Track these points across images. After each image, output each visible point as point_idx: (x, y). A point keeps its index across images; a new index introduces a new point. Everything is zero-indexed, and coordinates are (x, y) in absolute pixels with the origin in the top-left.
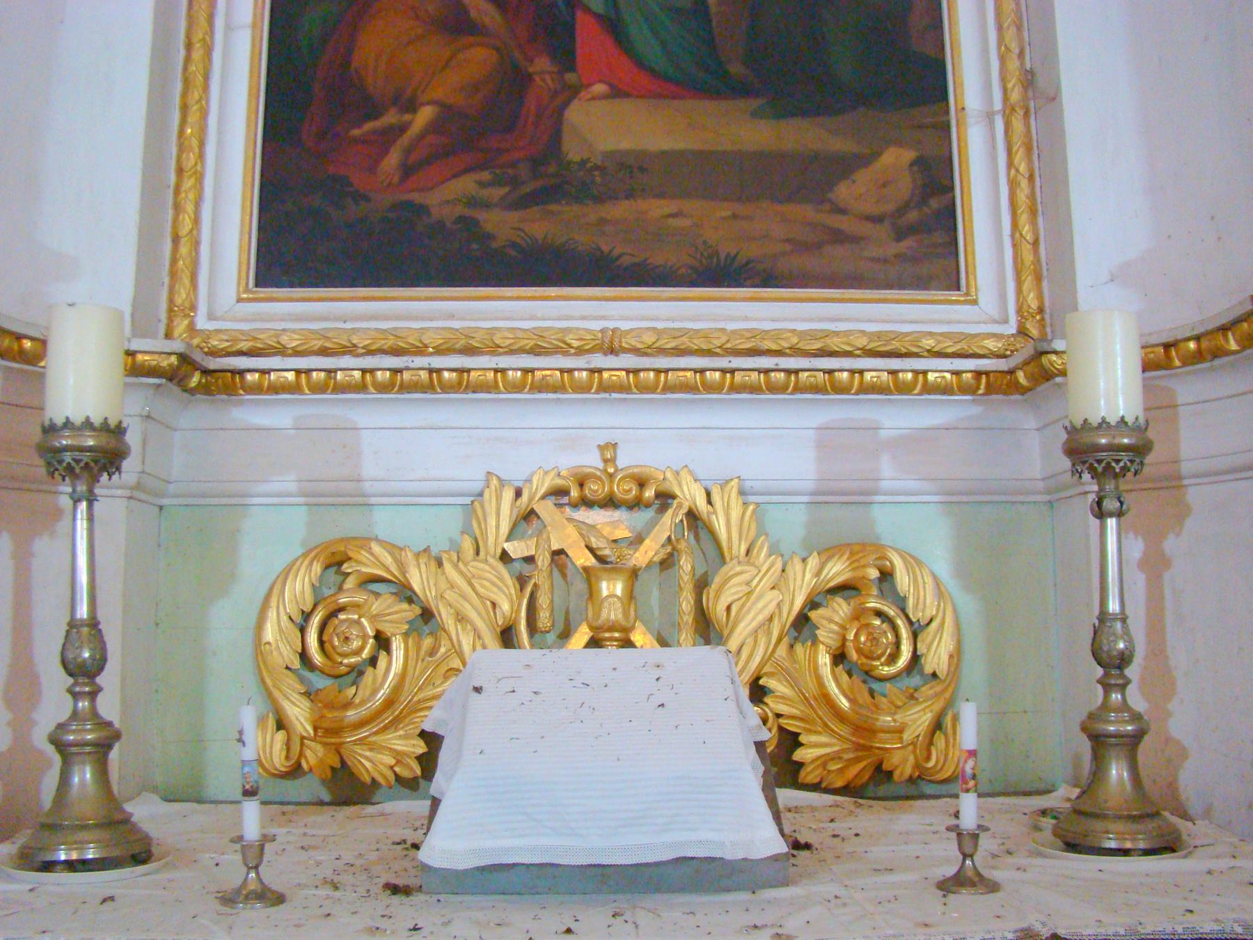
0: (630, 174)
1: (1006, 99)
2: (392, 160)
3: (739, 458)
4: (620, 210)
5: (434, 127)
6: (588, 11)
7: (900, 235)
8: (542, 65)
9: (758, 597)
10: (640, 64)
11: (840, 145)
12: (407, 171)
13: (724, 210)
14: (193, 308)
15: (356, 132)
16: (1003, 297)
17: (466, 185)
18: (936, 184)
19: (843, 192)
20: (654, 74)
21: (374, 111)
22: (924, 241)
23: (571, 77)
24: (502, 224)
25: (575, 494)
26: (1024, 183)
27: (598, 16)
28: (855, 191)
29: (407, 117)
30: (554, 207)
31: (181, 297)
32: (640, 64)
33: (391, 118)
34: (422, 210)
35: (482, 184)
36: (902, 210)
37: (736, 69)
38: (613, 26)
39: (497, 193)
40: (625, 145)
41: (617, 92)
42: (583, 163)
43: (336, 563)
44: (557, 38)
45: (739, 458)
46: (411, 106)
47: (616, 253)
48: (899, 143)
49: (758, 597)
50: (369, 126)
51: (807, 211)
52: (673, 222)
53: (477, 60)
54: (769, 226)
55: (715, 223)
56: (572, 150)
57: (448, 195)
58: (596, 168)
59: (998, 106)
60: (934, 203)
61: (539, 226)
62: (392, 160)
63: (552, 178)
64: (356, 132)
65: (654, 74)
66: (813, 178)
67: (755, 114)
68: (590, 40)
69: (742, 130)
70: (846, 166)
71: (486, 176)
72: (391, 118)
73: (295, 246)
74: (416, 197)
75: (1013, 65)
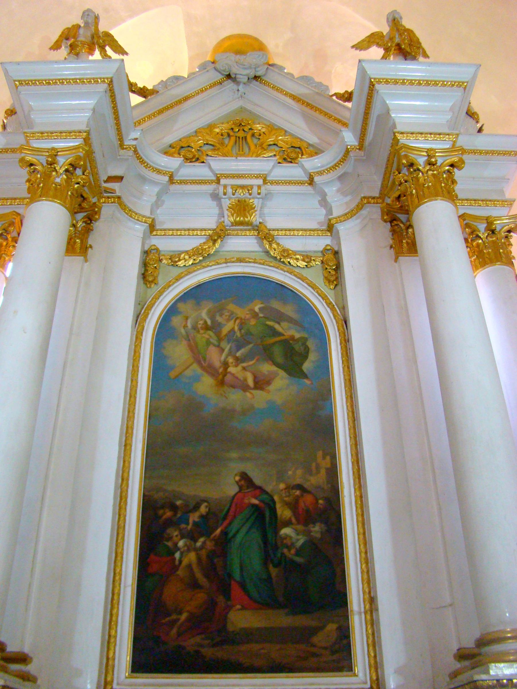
0: (248, 636)
1: (365, 608)
2: (174, 631)
4: (244, 648)
5: (187, 620)
6: (235, 580)
7: (333, 653)
8: (221, 599)
10: (251, 598)
11: (314, 623)
12: (179, 635)
13: (278, 647)
14: (112, 681)
15: (164, 621)
16: (366, 676)
17: (198, 639)
19: (315, 640)
20: (255, 601)
21: (169, 615)
23: (229, 603)
24: (208, 652)
26: (371, 637)
27: (237, 582)
28: (319, 639)
29: (179, 617)
30: (224, 647)
31: (109, 679)
32: (251, 598)
33: (174, 617)
34: (183, 648)
35: (203, 639)
36: (335, 643)
37: (281, 599)
38: (242, 585)
39: (206, 642)
40: (247, 625)
41: (244, 608)
42: (233, 632)
46: (181, 613)
47: (244, 661)
48: (333, 622)
50: (167, 619)
51: (303, 646)
52: (263, 651)
53: (201, 597)
54: (291, 651)
55: (273, 651)
56: (230, 627)
57: (192, 642)
58: (238, 633)
59: (363, 610)
60: (345, 642)
61: (220, 653)
62: (174, 631)
64: (164, 621)
65: (255, 601)
66: (305, 635)
67: (287, 614)
68: (236, 591)
69: (282, 619)
70: (316, 630)
71: (203, 636)
72: (174, 617)
74: (182, 643)
75: (367, 596)
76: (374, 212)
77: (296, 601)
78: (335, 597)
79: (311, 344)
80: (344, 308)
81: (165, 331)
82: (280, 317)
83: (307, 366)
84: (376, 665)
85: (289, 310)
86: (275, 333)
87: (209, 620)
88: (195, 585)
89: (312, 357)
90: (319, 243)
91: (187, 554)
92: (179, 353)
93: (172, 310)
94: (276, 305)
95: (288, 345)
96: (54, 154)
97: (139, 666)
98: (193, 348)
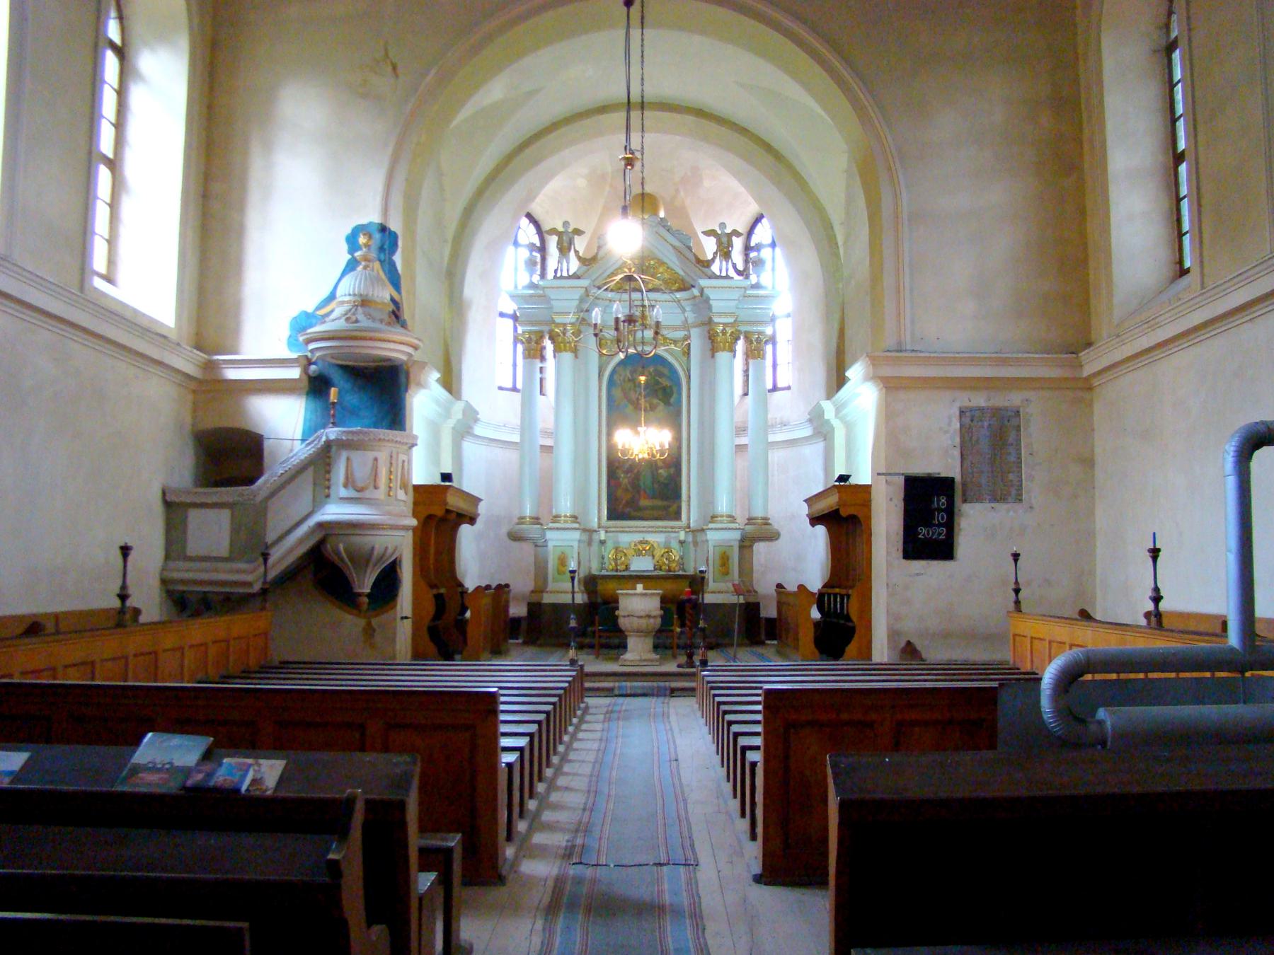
0: (645, 508)
3: (656, 539)
9: (658, 553)
18: (680, 508)
22: (677, 516)
24: (633, 514)
25: (641, 542)
43: (616, 549)
44: (638, 492)
45: (656, 539)
49: (658, 553)
55: (655, 513)
61: (638, 514)
63: (639, 509)
66: (666, 508)
69: (659, 503)
73: (611, 517)
76: (706, 328)
77: (663, 497)
78: (677, 495)
79: (675, 389)
80: (689, 370)
81: (611, 382)
82: (661, 375)
83: (672, 400)
84: (689, 519)
85: (666, 371)
86: (657, 383)
87: (633, 503)
88: (627, 490)
89: (675, 395)
90: (680, 334)
91: (624, 480)
92: (617, 393)
93: (614, 372)
94: (660, 368)
95: (664, 389)
96: (565, 325)
97: (609, 518)
98: (623, 390)
